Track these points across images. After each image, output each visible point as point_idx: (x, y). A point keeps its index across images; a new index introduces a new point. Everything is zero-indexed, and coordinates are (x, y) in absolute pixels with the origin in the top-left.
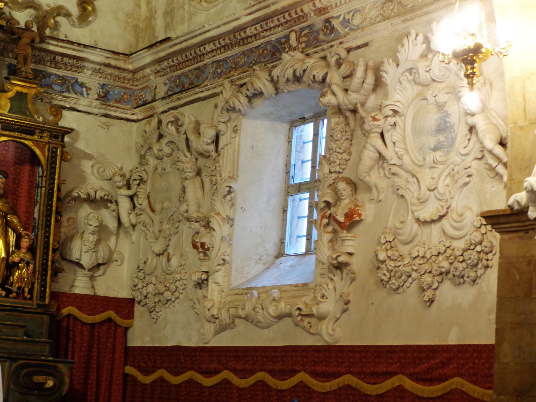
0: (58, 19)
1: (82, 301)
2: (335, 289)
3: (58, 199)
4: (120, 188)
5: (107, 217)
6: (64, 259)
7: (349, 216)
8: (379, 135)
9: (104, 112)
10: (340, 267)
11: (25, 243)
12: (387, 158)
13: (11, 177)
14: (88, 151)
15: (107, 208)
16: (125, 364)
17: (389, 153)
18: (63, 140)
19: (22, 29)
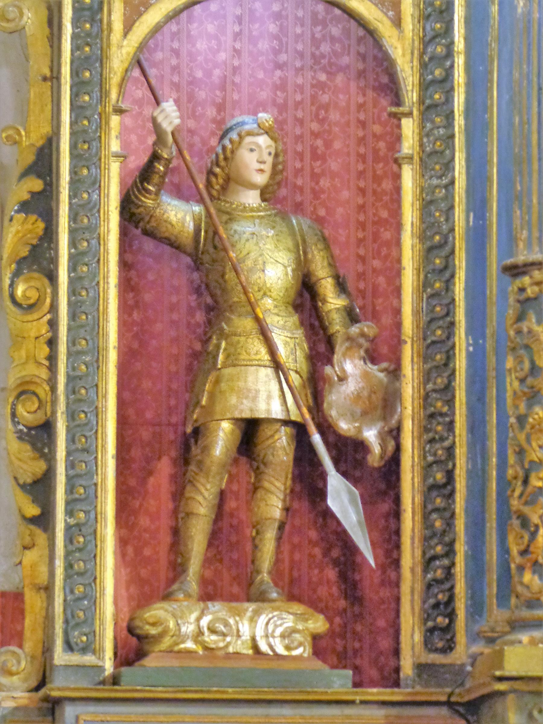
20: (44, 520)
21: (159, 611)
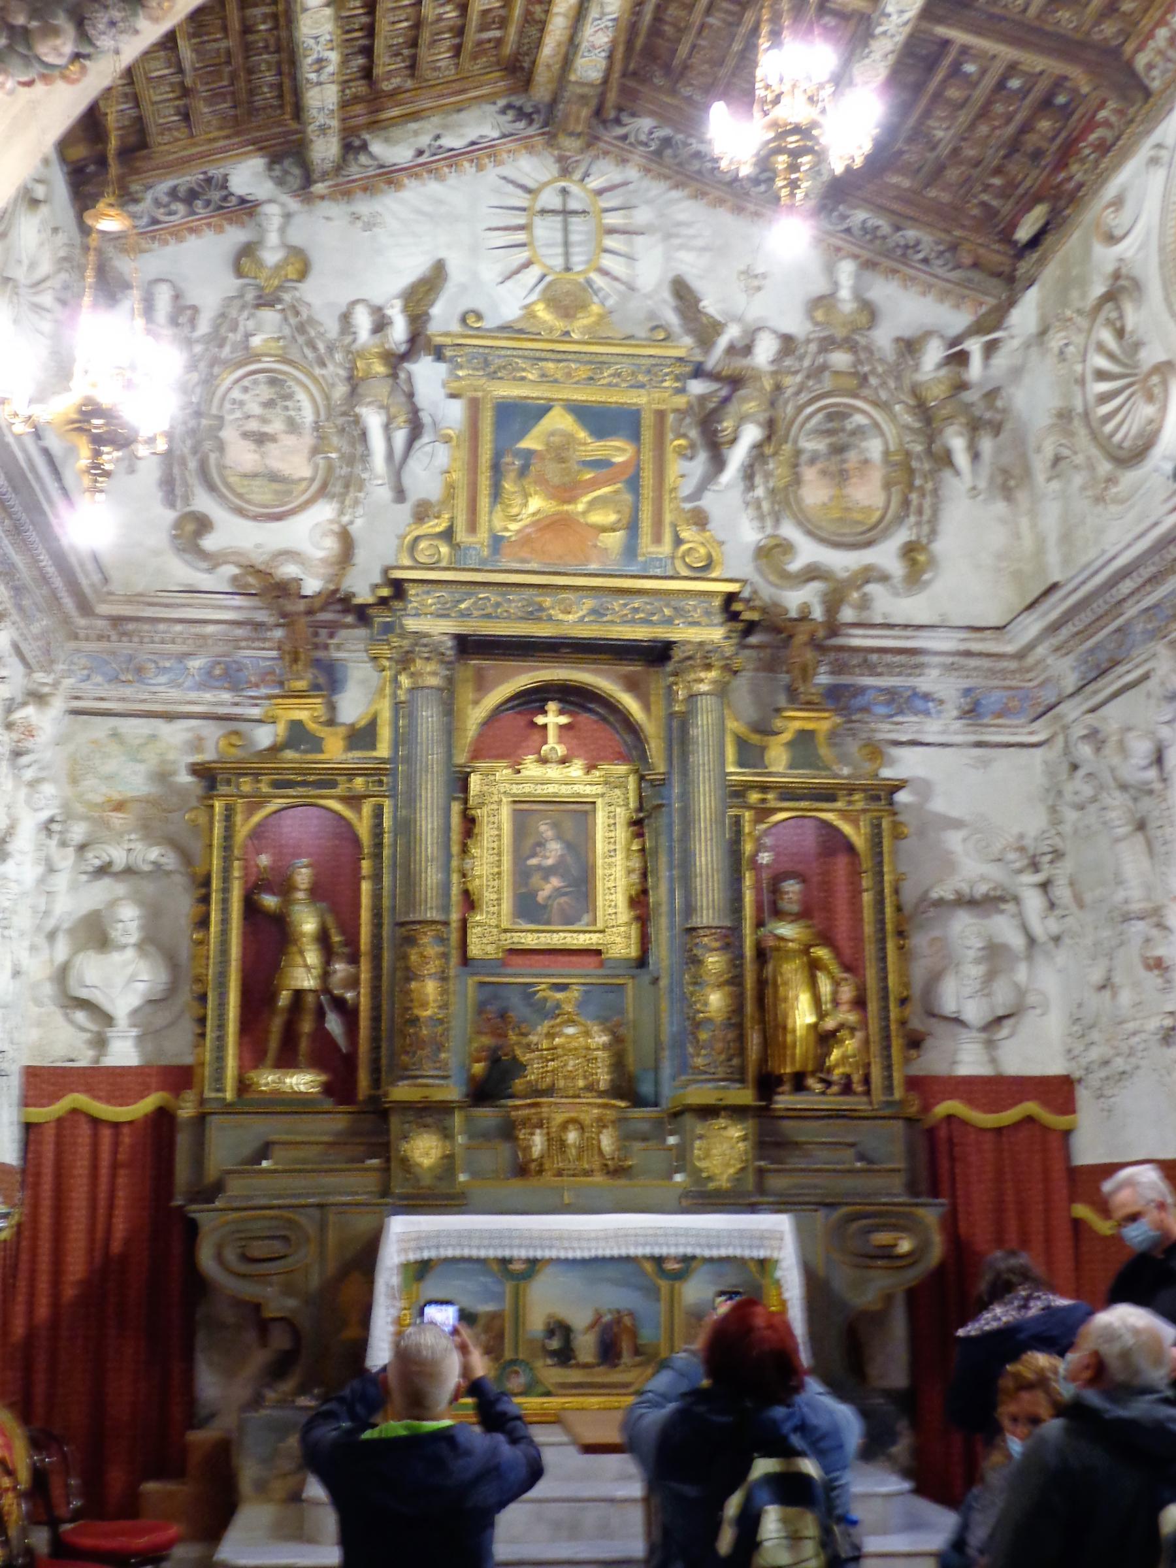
0: (871, 588)
1: (969, 1088)
3: (899, 909)
4: (1020, 871)
5: (1004, 929)
6: (934, 1015)
9: (973, 738)
11: (847, 993)
13: (815, 879)
14: (955, 813)
15: (1002, 912)
16: (1072, 1199)
18: (891, 803)
19: (795, 620)
20: (203, 1035)
21: (253, 1075)
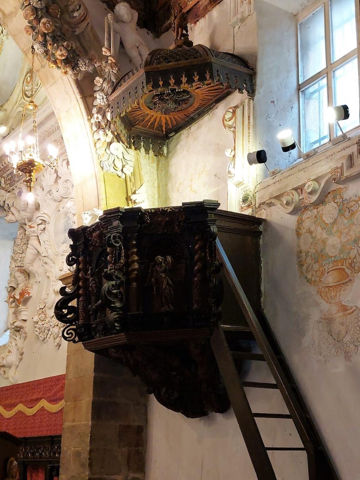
2: (16, 345)
7: (21, 294)
8: (37, 238)
10: (18, 330)
12: (41, 252)
17: (41, 249)
